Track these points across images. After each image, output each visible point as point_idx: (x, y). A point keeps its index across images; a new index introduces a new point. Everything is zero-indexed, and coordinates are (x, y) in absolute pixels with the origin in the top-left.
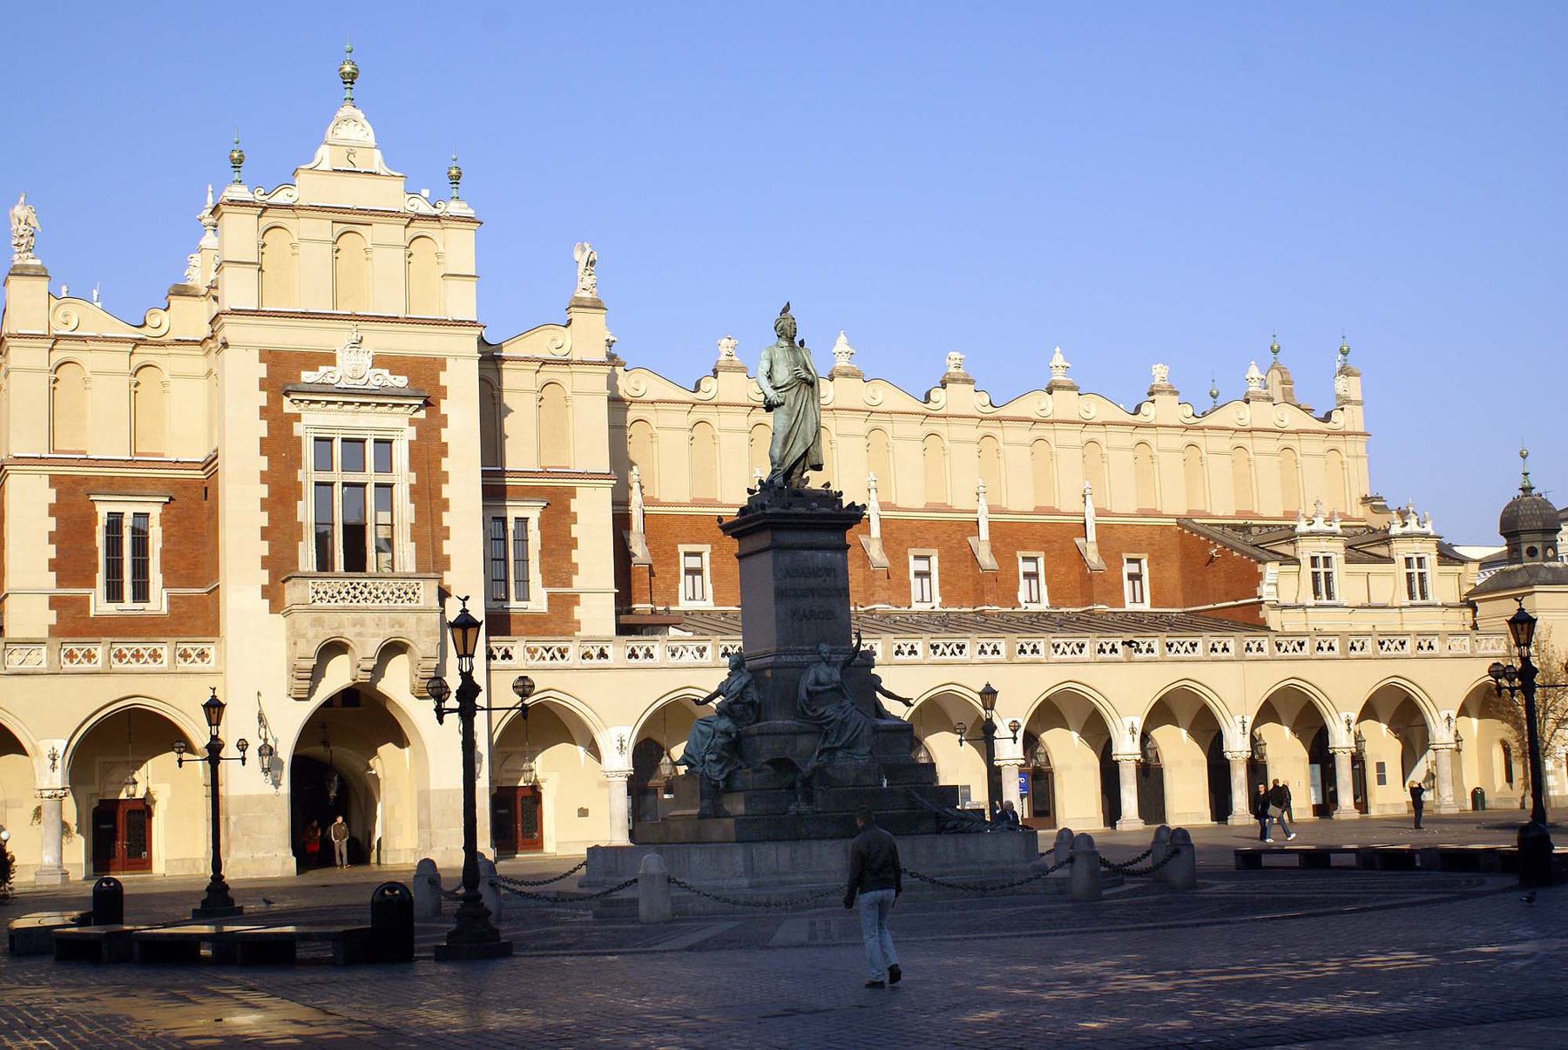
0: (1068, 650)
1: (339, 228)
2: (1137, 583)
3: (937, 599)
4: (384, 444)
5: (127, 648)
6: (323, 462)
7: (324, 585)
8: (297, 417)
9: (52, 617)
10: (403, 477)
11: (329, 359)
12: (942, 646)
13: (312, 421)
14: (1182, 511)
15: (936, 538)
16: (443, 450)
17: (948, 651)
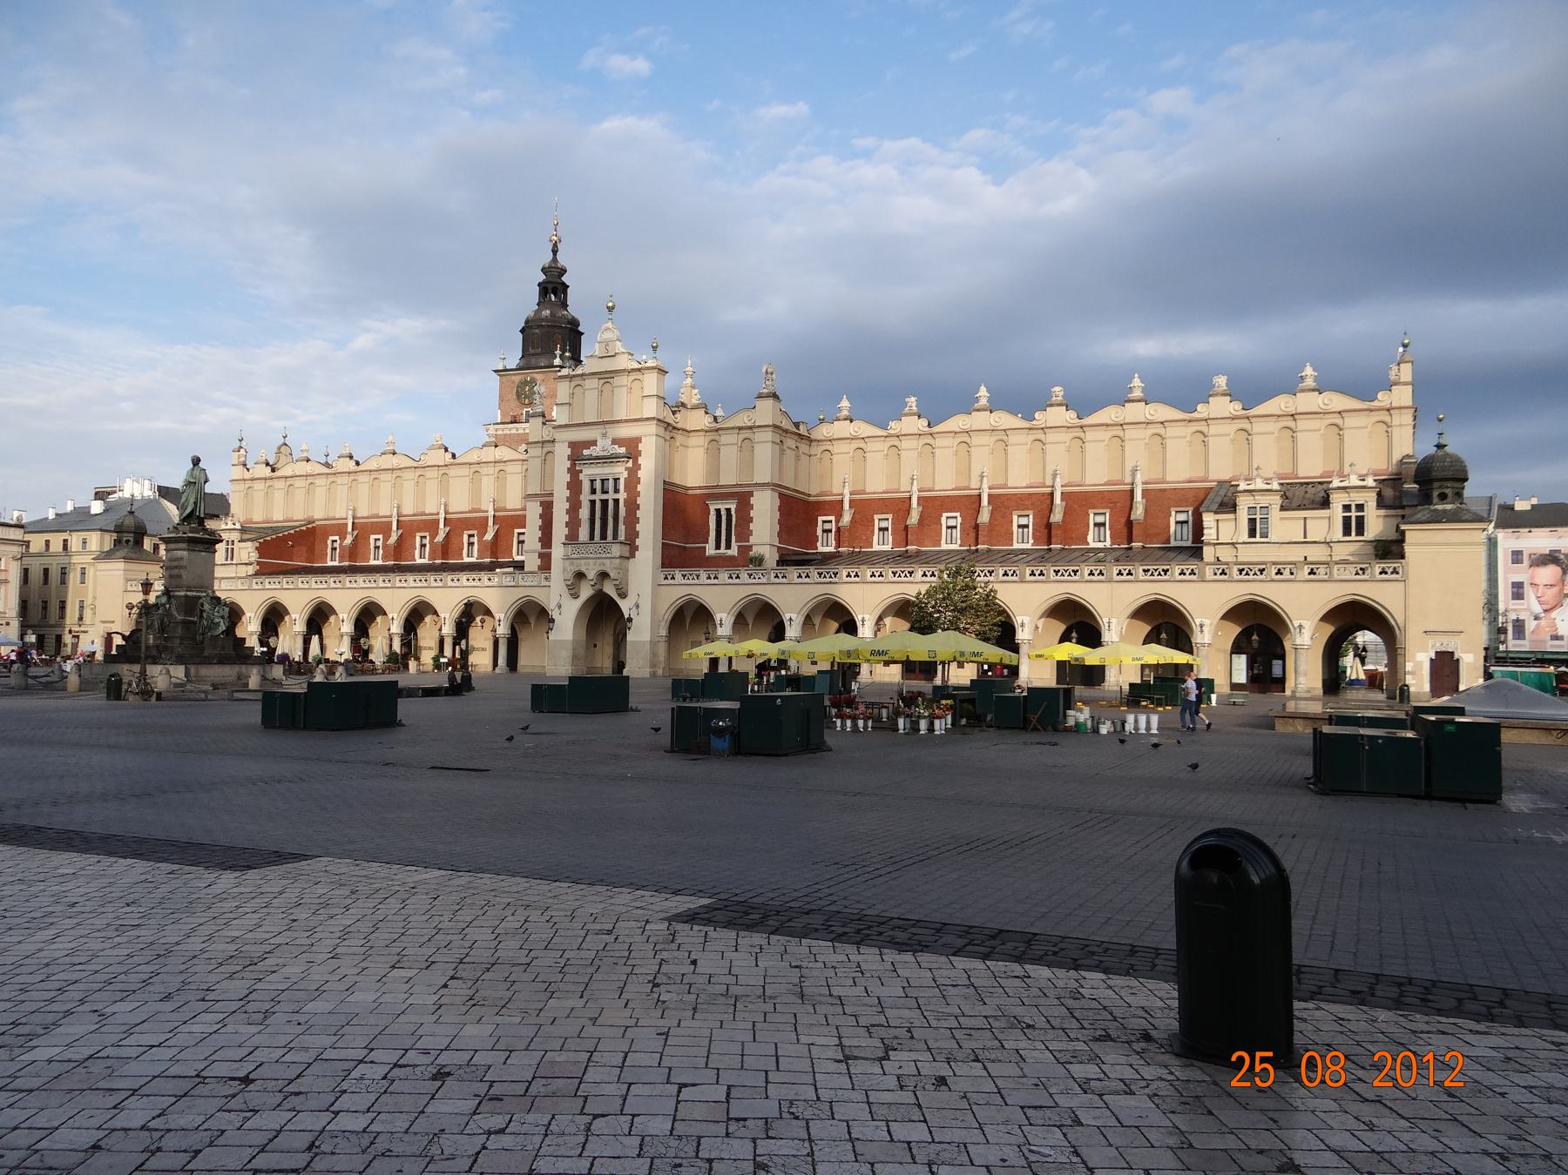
0: (903, 575)
1: (603, 381)
2: (1102, 529)
3: (1031, 541)
4: (616, 480)
5: (455, 577)
6: (593, 491)
7: (592, 548)
8: (581, 471)
9: (539, 562)
10: (622, 496)
11: (594, 443)
12: (899, 572)
13: (587, 473)
14: (1226, 477)
15: (1032, 504)
16: (638, 481)
17: (903, 575)
